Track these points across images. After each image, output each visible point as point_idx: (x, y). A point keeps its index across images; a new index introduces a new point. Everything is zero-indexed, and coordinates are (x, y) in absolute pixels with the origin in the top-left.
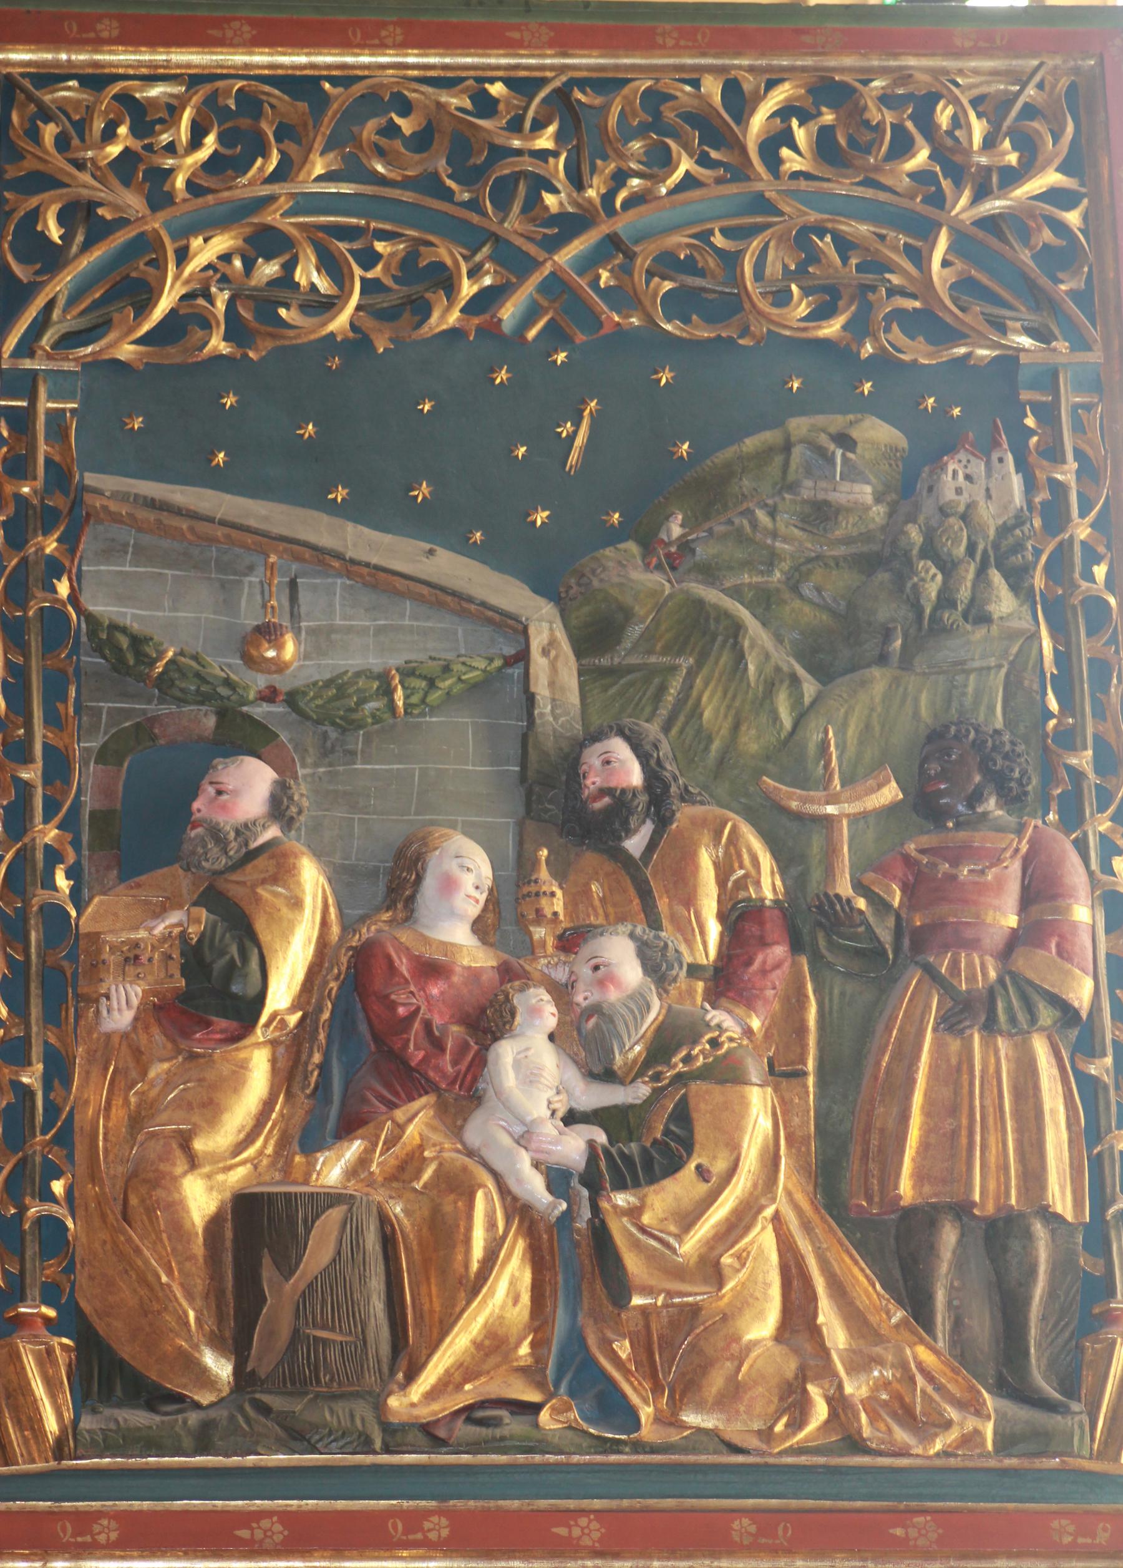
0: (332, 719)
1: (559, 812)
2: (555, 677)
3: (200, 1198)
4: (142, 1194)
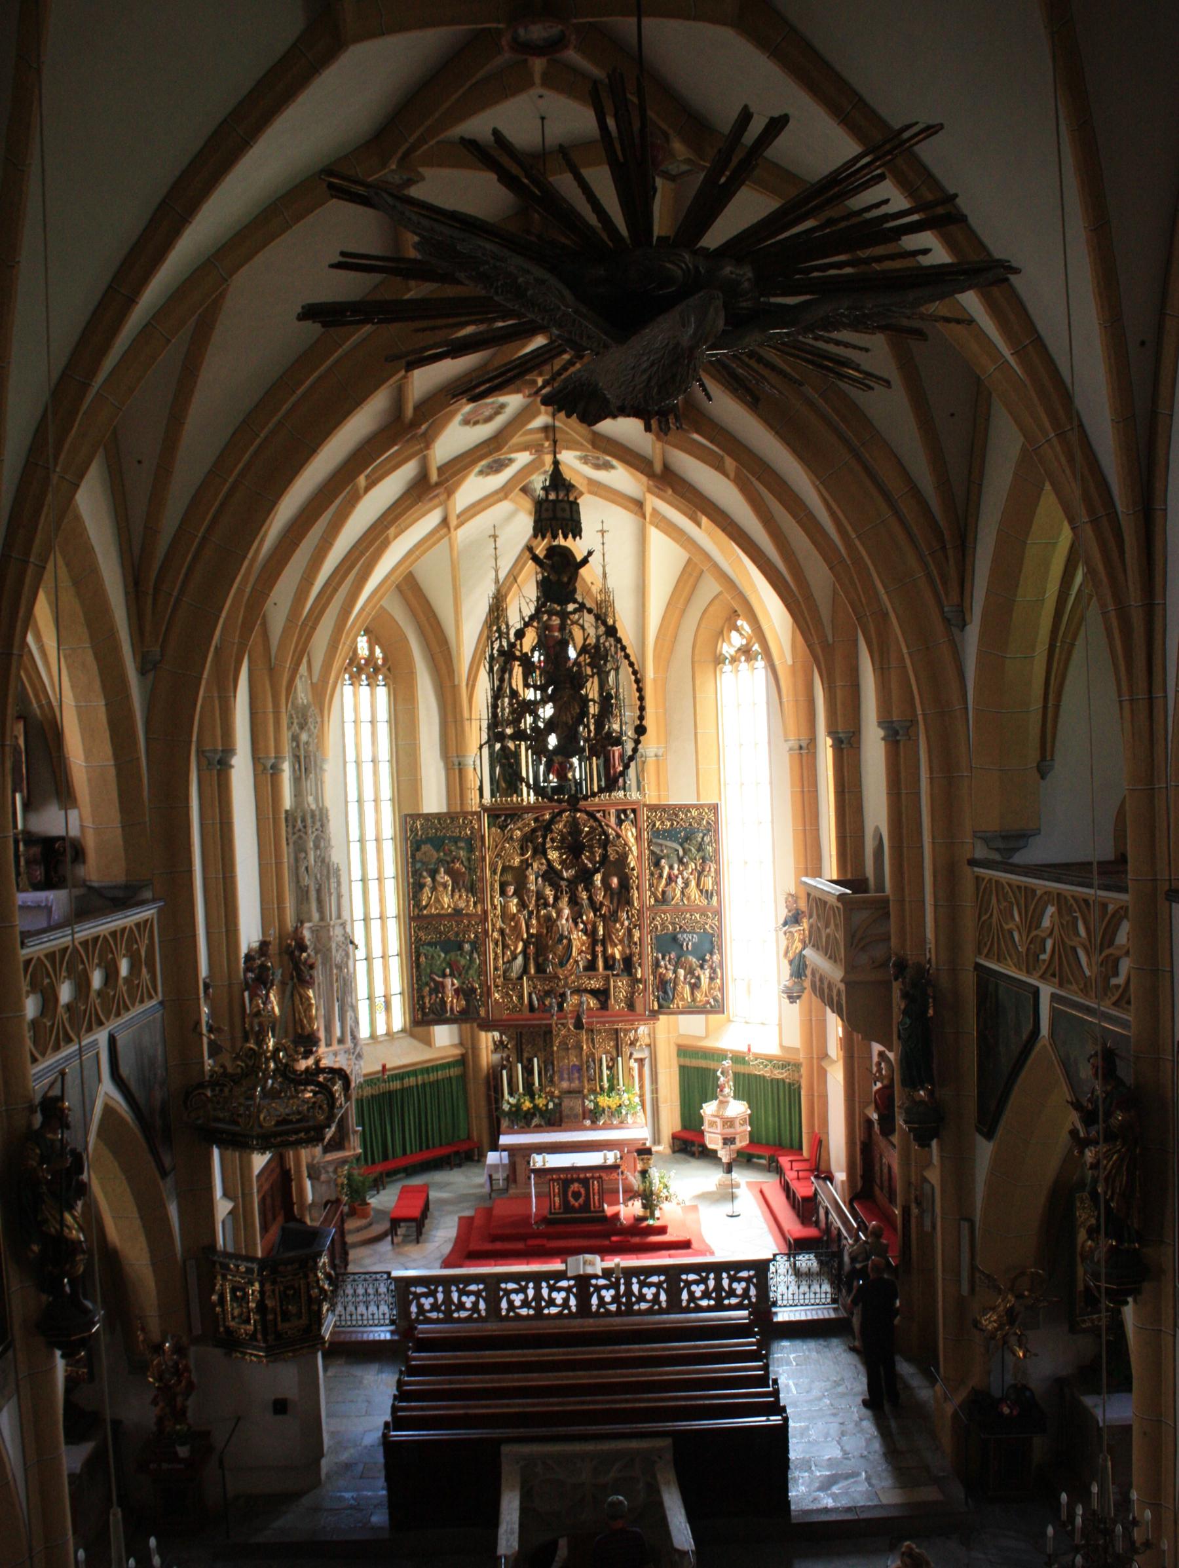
1: (681, 861)
2: (681, 853)
4: (657, 889)
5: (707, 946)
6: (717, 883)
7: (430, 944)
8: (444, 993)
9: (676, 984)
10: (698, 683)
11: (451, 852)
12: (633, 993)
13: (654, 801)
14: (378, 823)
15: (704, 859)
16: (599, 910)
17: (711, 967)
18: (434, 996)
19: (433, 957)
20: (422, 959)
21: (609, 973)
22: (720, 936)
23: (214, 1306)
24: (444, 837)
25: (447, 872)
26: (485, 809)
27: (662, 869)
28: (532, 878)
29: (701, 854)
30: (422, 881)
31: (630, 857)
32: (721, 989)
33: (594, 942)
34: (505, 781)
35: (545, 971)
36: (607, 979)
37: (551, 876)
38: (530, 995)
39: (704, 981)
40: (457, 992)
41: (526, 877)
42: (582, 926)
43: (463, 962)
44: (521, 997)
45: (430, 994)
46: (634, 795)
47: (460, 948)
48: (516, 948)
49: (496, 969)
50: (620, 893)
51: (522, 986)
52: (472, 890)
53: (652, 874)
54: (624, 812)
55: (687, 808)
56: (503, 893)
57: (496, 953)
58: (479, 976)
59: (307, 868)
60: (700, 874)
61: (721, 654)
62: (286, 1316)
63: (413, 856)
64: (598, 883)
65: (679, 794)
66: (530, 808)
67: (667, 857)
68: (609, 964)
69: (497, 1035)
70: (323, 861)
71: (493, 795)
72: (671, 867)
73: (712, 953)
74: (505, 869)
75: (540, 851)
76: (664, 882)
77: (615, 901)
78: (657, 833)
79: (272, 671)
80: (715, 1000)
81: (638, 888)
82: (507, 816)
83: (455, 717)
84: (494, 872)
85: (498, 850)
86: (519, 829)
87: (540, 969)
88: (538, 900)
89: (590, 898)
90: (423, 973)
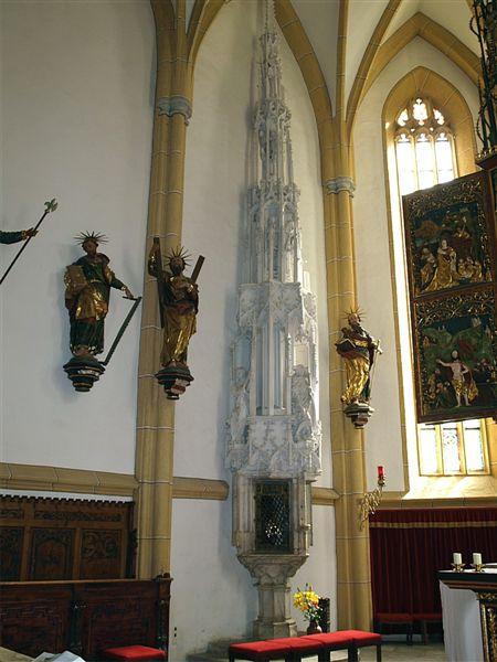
43: (474, 341)
47: (470, 325)
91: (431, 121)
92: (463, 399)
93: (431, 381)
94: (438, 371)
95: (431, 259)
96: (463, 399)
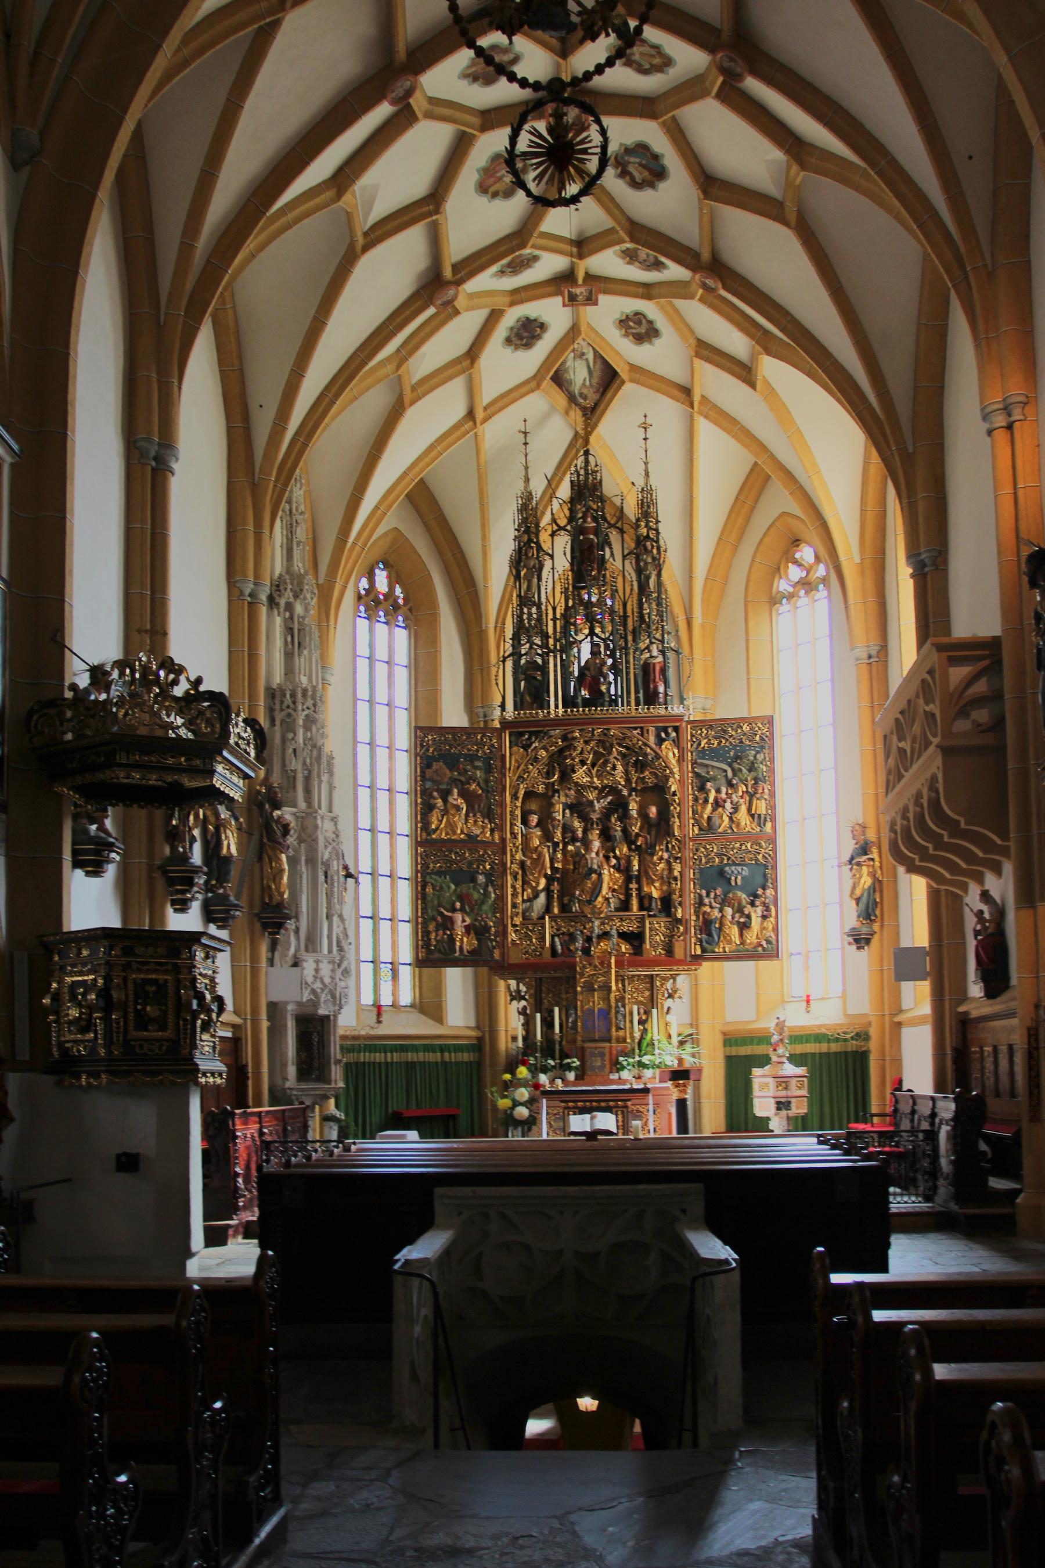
0: (713, 779)
1: (730, 784)
2: (730, 774)
3: (705, 816)
4: (701, 817)
5: (759, 880)
6: (772, 807)
7: (439, 873)
8: (452, 929)
9: (721, 924)
10: (751, 624)
11: (466, 771)
12: (673, 936)
13: (699, 717)
14: (391, 772)
15: (756, 780)
16: (634, 843)
17: (764, 904)
18: (441, 932)
19: (441, 888)
20: (429, 890)
21: (644, 913)
22: (775, 867)
23: (46, 1011)
24: (460, 755)
25: (461, 794)
26: (505, 724)
27: (707, 792)
28: (559, 807)
29: (753, 774)
30: (432, 801)
31: (671, 780)
32: (776, 929)
33: (628, 879)
34: (530, 695)
35: (571, 911)
36: (642, 921)
37: (579, 808)
38: (553, 937)
39: (756, 922)
40: (468, 929)
41: (552, 805)
42: (614, 861)
43: (476, 896)
44: (542, 938)
45: (437, 930)
46: (676, 709)
47: (474, 880)
48: (538, 884)
49: (514, 906)
50: (658, 825)
51: (543, 927)
52: (489, 815)
53: (696, 800)
54: (665, 729)
55: (737, 723)
56: (525, 822)
57: (513, 887)
58: (494, 913)
59: (295, 750)
60: (751, 796)
61: (778, 592)
62: (142, 1020)
63: (423, 773)
64: (634, 813)
65: (729, 707)
66: (557, 722)
67: (713, 779)
68: (645, 903)
69: (513, 983)
70: (314, 746)
71: (515, 709)
72: (718, 791)
73: (764, 889)
74: (529, 795)
75: (566, 775)
76: (709, 807)
77: (653, 833)
78: (702, 753)
79: (256, 489)
80: (769, 942)
81: (679, 817)
82: (531, 733)
83: (481, 664)
84: (515, 797)
85: (521, 771)
86: (544, 748)
87: (564, 908)
88: (563, 833)
89: (625, 831)
90: (430, 905)
91: (390, 595)
92: (461, 948)
93: (431, 927)
94: (439, 919)
95: (439, 802)
96: (461, 948)
